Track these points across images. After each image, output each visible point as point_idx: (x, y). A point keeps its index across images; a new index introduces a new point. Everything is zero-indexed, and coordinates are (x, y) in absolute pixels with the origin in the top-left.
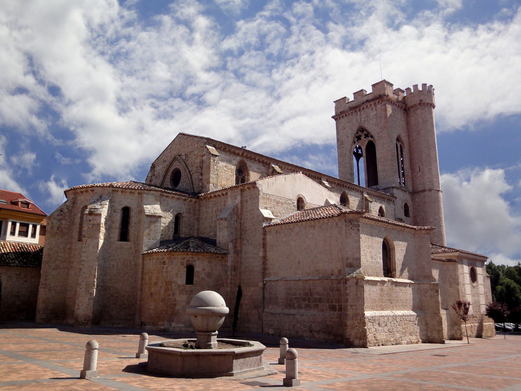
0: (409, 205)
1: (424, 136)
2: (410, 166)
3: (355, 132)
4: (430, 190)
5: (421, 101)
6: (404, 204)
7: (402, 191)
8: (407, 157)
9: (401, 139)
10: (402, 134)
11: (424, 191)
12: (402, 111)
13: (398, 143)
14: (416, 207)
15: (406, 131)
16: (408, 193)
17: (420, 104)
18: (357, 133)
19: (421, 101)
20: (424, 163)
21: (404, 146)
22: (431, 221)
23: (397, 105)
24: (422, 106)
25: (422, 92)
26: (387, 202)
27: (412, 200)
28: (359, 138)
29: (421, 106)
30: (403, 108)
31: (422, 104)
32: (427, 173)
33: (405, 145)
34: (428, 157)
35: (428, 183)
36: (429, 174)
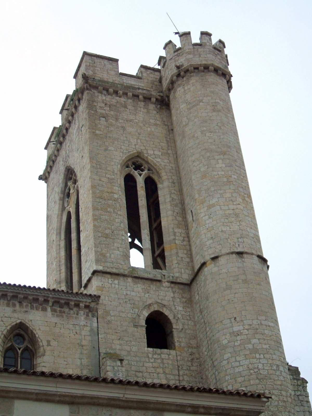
0: (171, 317)
1: (194, 136)
2: (180, 219)
3: (62, 185)
4: (215, 258)
5: (178, 67)
6: (146, 314)
7: (137, 280)
8: (168, 200)
9: (147, 162)
10: (150, 152)
11: (203, 264)
12: (152, 106)
13: (136, 173)
14: (198, 317)
15: (164, 144)
16: (167, 284)
17: (178, 75)
18: (66, 185)
19: (178, 67)
20: (197, 196)
21: (160, 177)
22: (225, 342)
23: (130, 94)
24: (185, 79)
25: (179, 52)
26: (54, 311)
27: (189, 302)
28: (69, 195)
29: (183, 77)
30: (153, 100)
31: (182, 73)
32: (207, 217)
33: (163, 174)
34: (205, 180)
35: (208, 243)
36: (210, 218)
